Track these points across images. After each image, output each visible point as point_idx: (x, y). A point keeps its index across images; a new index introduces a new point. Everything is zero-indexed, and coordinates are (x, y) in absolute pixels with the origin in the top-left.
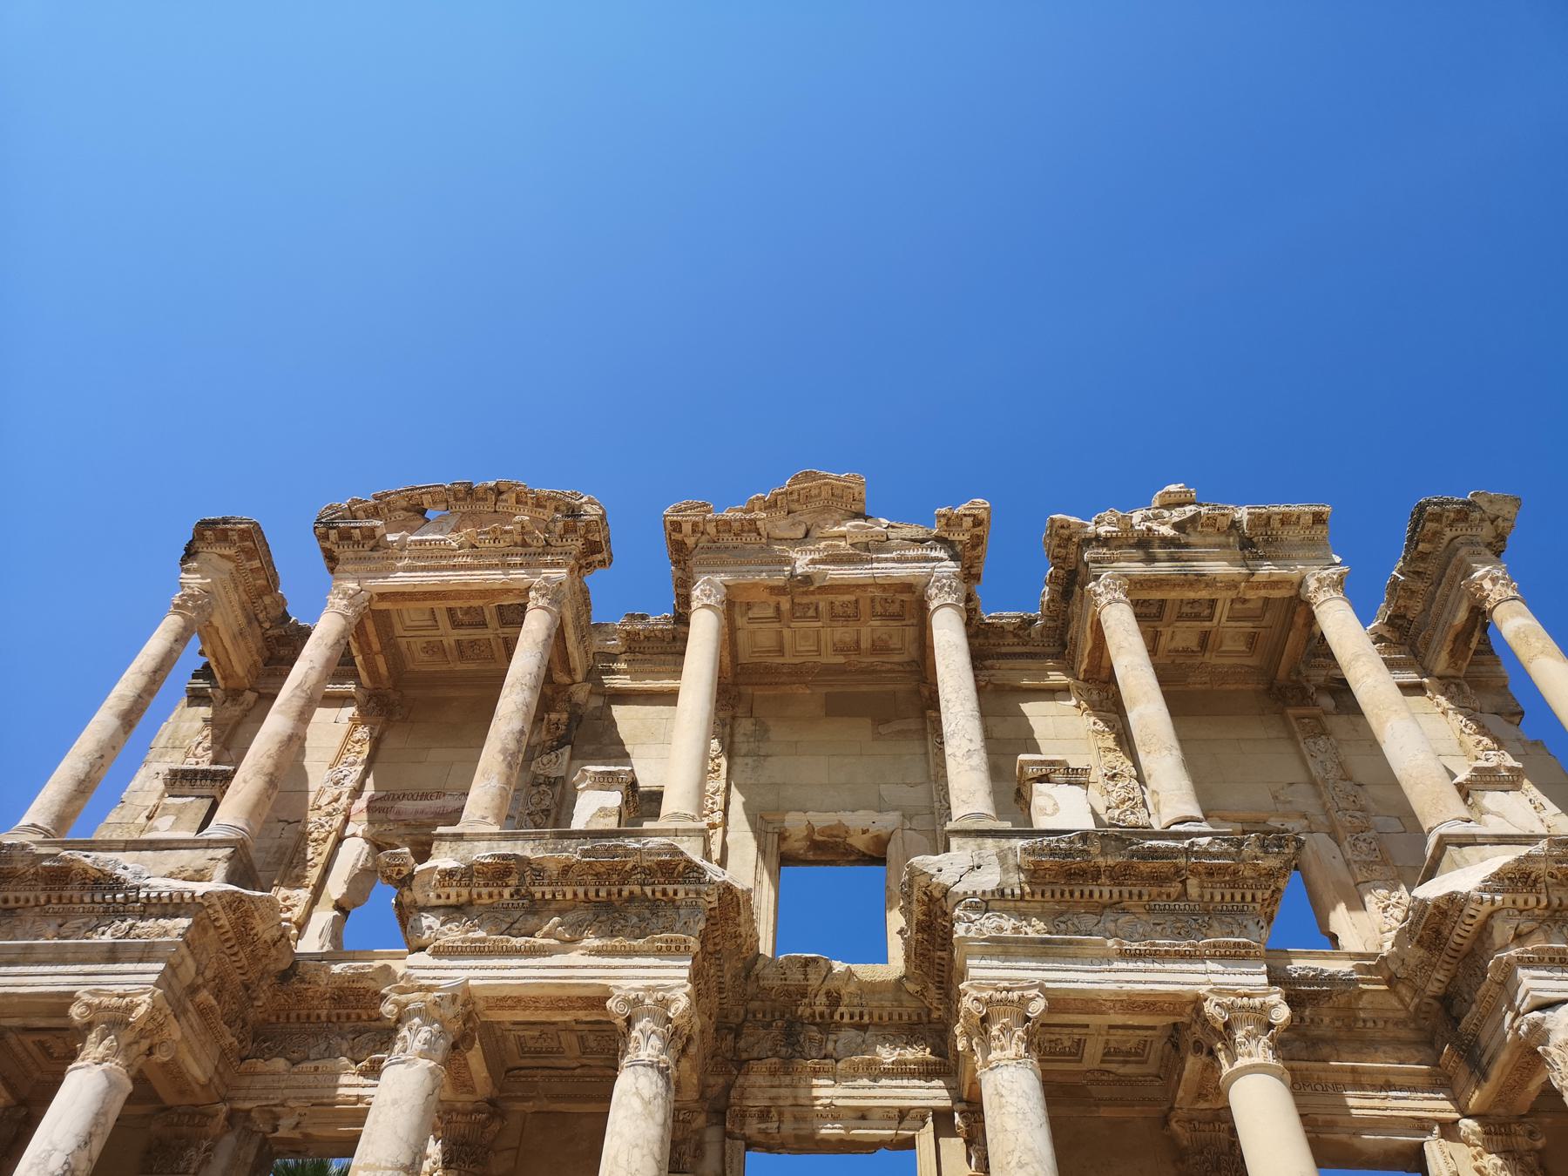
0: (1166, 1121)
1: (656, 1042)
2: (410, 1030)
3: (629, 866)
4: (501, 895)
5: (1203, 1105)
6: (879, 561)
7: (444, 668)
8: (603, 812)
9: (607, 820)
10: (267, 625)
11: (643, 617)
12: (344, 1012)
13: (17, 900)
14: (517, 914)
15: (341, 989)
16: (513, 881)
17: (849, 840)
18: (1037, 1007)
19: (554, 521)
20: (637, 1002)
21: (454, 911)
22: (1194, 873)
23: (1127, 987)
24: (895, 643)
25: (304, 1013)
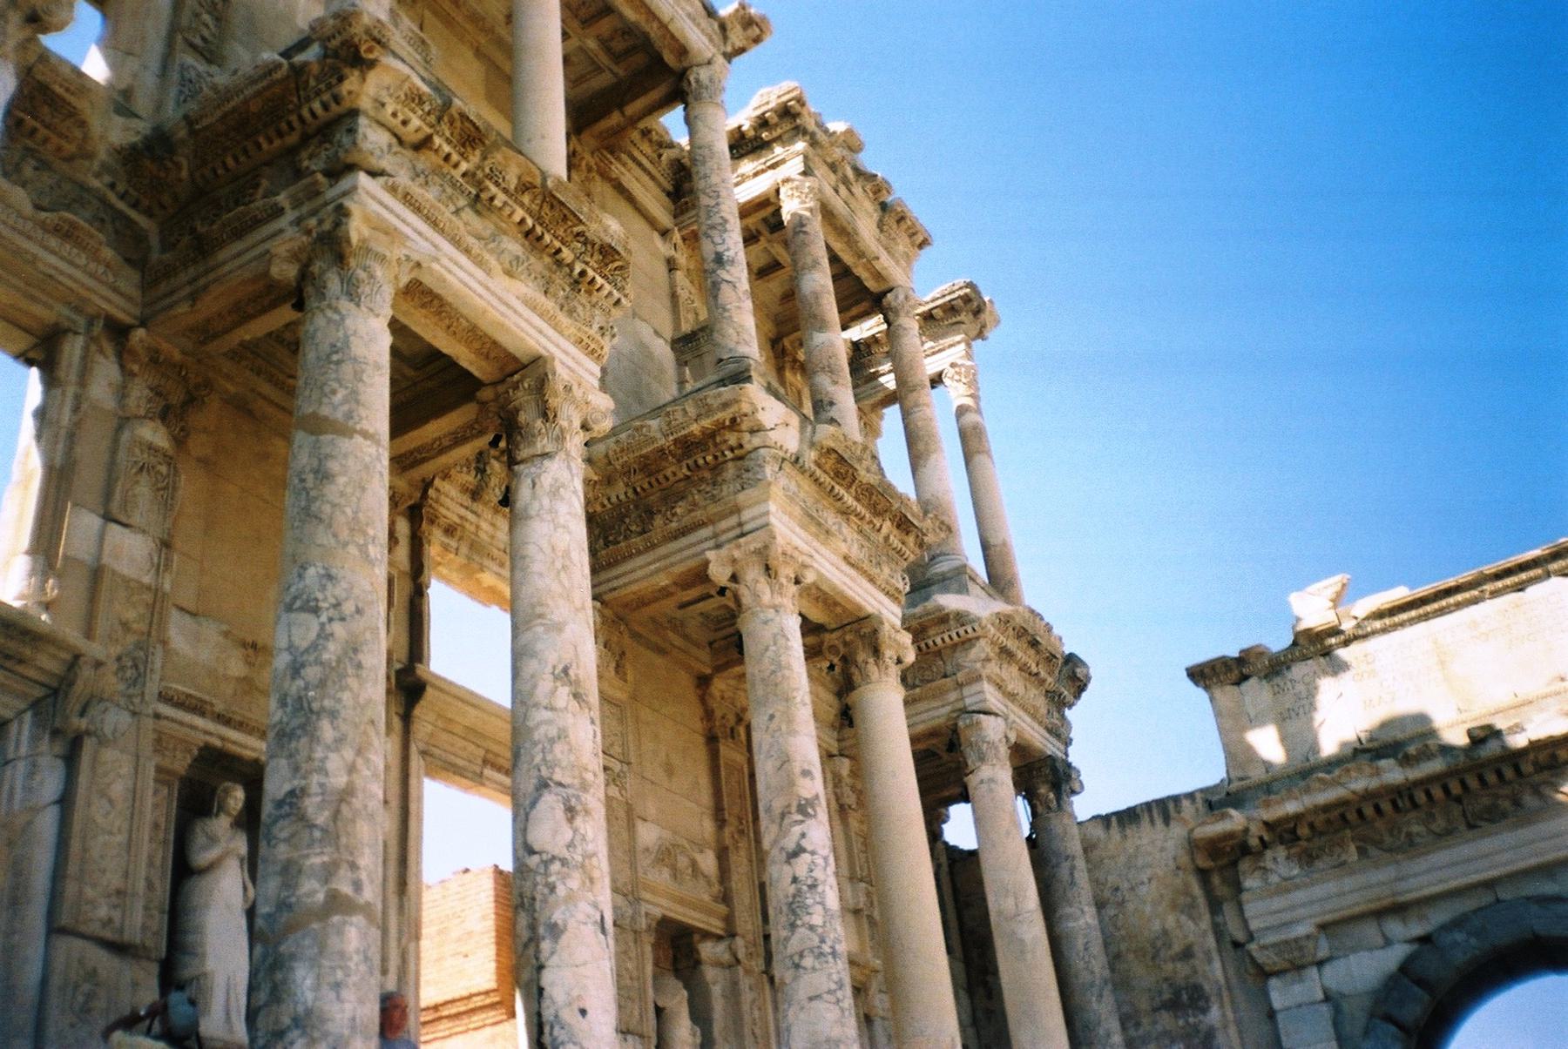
0: (703, 682)
4: (456, 166)
16: (475, 158)
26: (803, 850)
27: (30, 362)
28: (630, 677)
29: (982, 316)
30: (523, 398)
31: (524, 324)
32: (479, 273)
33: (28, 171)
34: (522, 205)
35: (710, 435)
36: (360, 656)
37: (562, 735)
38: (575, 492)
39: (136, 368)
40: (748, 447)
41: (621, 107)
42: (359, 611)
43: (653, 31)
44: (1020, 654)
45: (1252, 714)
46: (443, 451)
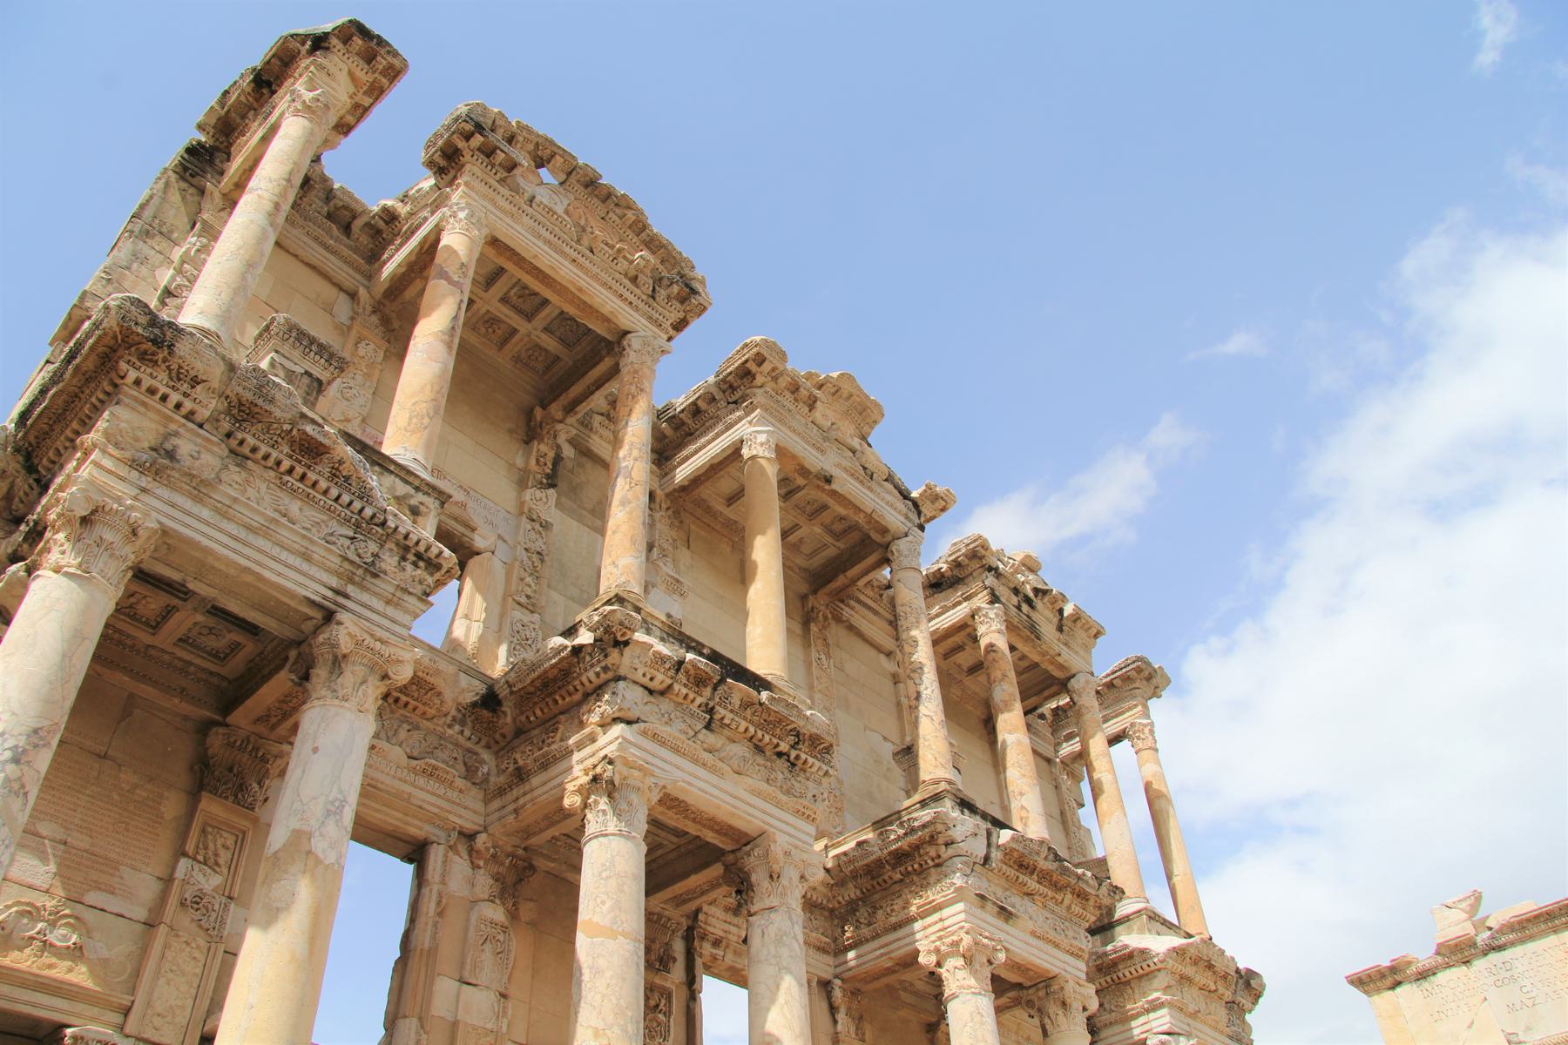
12: (404, 698)
13: (254, 450)
16: (708, 691)
20: (787, 853)
23: (1032, 958)
27: (410, 861)
28: (867, 1036)
29: (1154, 681)
30: (752, 861)
31: (751, 810)
32: (714, 779)
33: (403, 734)
34: (745, 719)
35: (916, 847)
38: (795, 937)
39: (481, 863)
41: (844, 571)
43: (861, 519)
46: (703, 893)
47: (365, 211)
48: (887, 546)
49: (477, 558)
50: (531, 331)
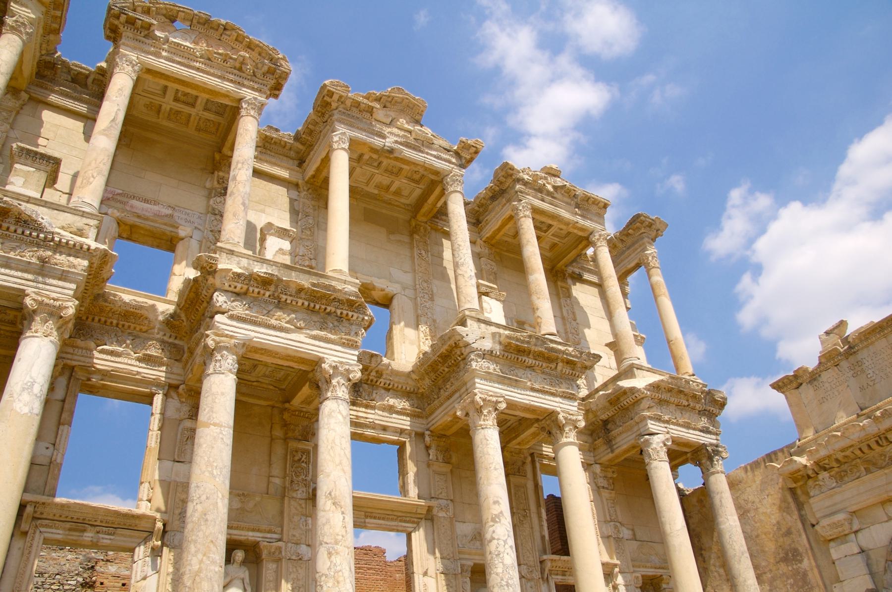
1: (344, 388)
2: (222, 356)
3: (332, 297)
4: (264, 295)
5: (518, 447)
6: (427, 154)
7: (154, 120)
8: (281, 251)
9: (285, 257)
10: (43, 52)
11: (277, 130)
12: (127, 324)
14: (271, 307)
15: (127, 311)
16: (272, 288)
17: (373, 292)
18: (503, 406)
19: (264, 64)
20: (335, 368)
21: (238, 295)
22: (562, 361)
23: (532, 403)
24: (405, 193)
25: (103, 319)
26: (494, 539)
32: (283, 334)
34: (301, 298)
36: (207, 516)
37: (328, 521)
40: (465, 354)
42: (207, 498)
44: (672, 399)
45: (806, 402)
47: (91, 72)
48: (442, 181)
49: (181, 242)
50: (196, 112)
